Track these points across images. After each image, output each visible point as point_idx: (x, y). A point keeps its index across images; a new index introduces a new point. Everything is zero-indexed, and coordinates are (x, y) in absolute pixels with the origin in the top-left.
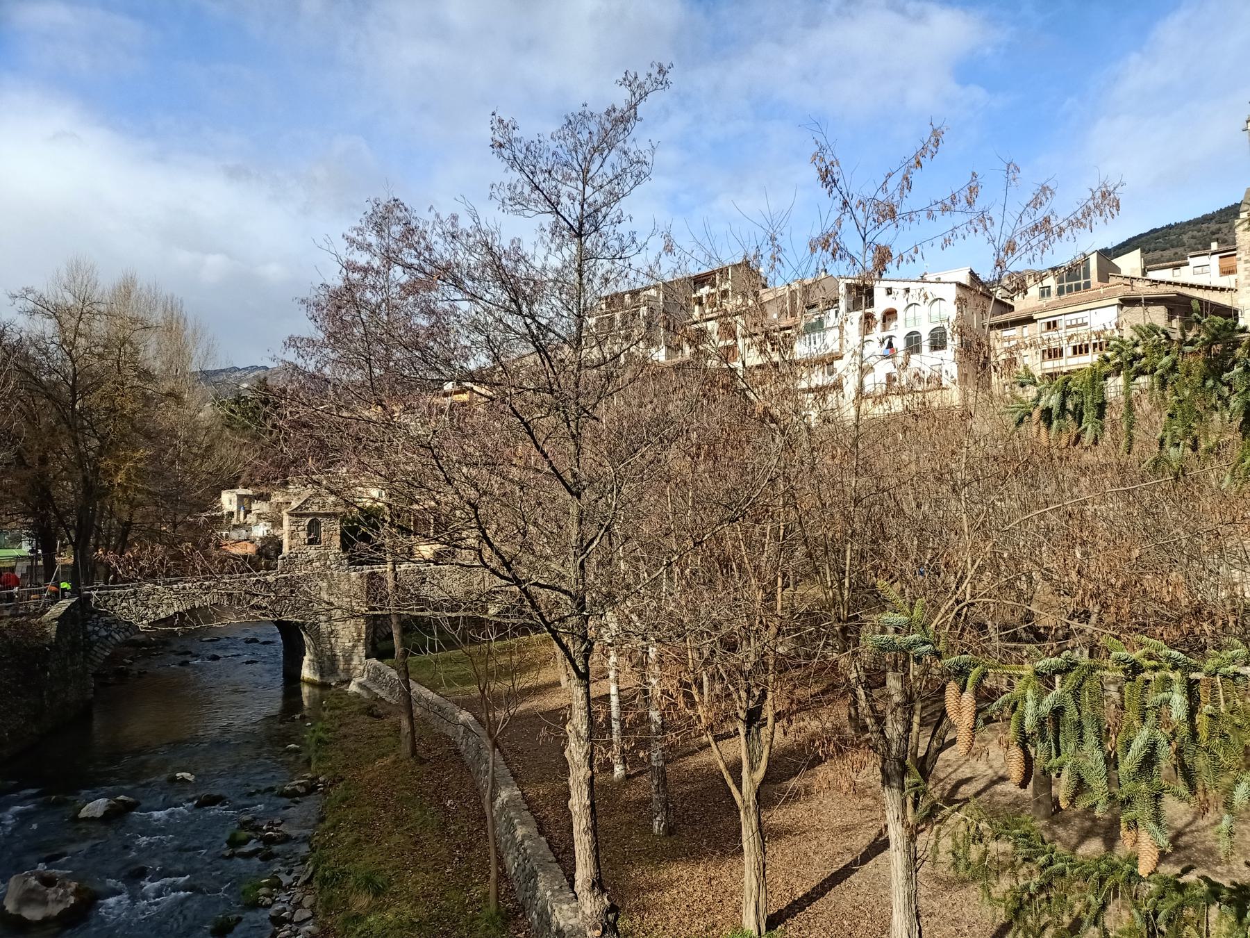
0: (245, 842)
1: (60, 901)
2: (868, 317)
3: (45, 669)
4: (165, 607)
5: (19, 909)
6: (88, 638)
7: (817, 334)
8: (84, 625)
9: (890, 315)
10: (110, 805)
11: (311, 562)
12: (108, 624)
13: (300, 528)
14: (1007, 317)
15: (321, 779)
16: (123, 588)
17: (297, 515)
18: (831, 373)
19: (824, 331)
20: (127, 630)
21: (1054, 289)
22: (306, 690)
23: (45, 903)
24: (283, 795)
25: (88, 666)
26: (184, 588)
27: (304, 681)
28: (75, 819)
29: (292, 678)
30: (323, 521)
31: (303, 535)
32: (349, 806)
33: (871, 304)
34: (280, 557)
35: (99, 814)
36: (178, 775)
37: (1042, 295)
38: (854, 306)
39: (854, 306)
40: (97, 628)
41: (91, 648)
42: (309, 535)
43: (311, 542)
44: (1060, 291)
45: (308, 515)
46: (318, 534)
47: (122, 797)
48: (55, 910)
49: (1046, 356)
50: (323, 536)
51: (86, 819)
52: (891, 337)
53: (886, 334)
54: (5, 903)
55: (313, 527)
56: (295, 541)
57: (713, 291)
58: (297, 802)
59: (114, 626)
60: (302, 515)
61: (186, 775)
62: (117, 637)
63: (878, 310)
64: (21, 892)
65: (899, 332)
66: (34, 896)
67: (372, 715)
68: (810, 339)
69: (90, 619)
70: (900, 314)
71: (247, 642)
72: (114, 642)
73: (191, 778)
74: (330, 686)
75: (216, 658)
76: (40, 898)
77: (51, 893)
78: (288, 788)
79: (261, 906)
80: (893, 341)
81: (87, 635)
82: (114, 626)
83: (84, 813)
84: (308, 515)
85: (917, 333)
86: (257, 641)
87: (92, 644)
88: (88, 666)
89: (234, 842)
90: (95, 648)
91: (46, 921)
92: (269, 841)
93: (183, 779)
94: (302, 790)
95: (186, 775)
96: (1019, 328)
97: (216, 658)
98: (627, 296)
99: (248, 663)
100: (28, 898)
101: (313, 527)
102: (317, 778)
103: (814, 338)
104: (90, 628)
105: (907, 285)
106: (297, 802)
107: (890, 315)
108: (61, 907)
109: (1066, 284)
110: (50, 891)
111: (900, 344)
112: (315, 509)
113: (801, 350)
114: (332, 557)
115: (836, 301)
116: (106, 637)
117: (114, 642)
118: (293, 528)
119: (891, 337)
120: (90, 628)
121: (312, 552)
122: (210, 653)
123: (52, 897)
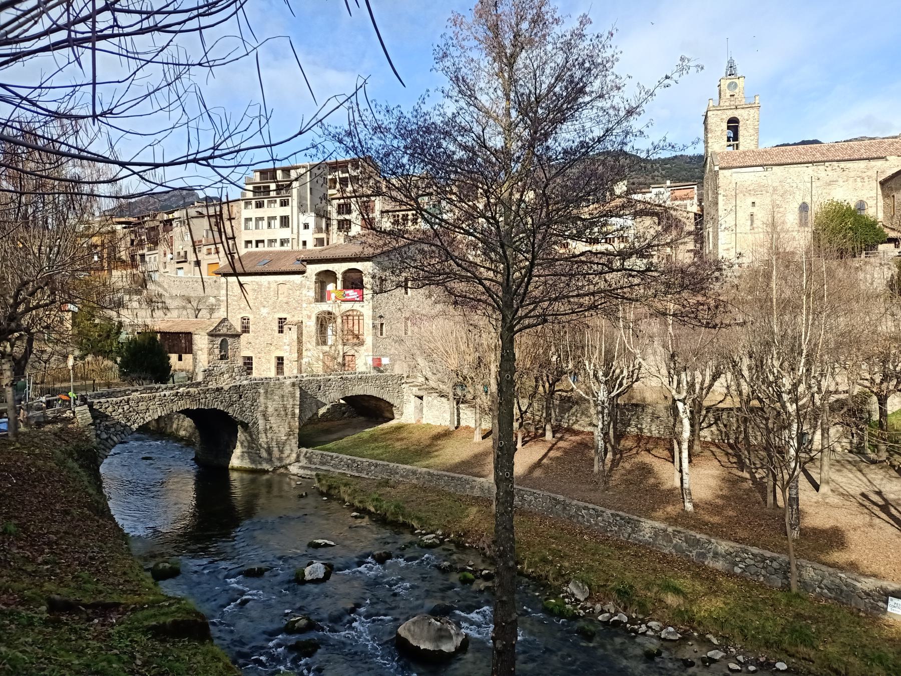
0: (472, 582)
11: (222, 373)
12: (107, 428)
20: (123, 433)
22: (234, 476)
23: (450, 637)
26: (165, 395)
30: (230, 341)
31: (217, 351)
43: (223, 358)
45: (220, 336)
46: (226, 351)
50: (230, 353)
51: (313, 581)
59: (113, 430)
62: (115, 439)
66: (443, 633)
72: (112, 443)
73: (332, 543)
76: (447, 634)
83: (308, 577)
84: (220, 336)
93: (326, 545)
108: (460, 639)
112: (224, 331)
116: (106, 439)
117: (112, 443)
118: (211, 346)
121: (223, 365)
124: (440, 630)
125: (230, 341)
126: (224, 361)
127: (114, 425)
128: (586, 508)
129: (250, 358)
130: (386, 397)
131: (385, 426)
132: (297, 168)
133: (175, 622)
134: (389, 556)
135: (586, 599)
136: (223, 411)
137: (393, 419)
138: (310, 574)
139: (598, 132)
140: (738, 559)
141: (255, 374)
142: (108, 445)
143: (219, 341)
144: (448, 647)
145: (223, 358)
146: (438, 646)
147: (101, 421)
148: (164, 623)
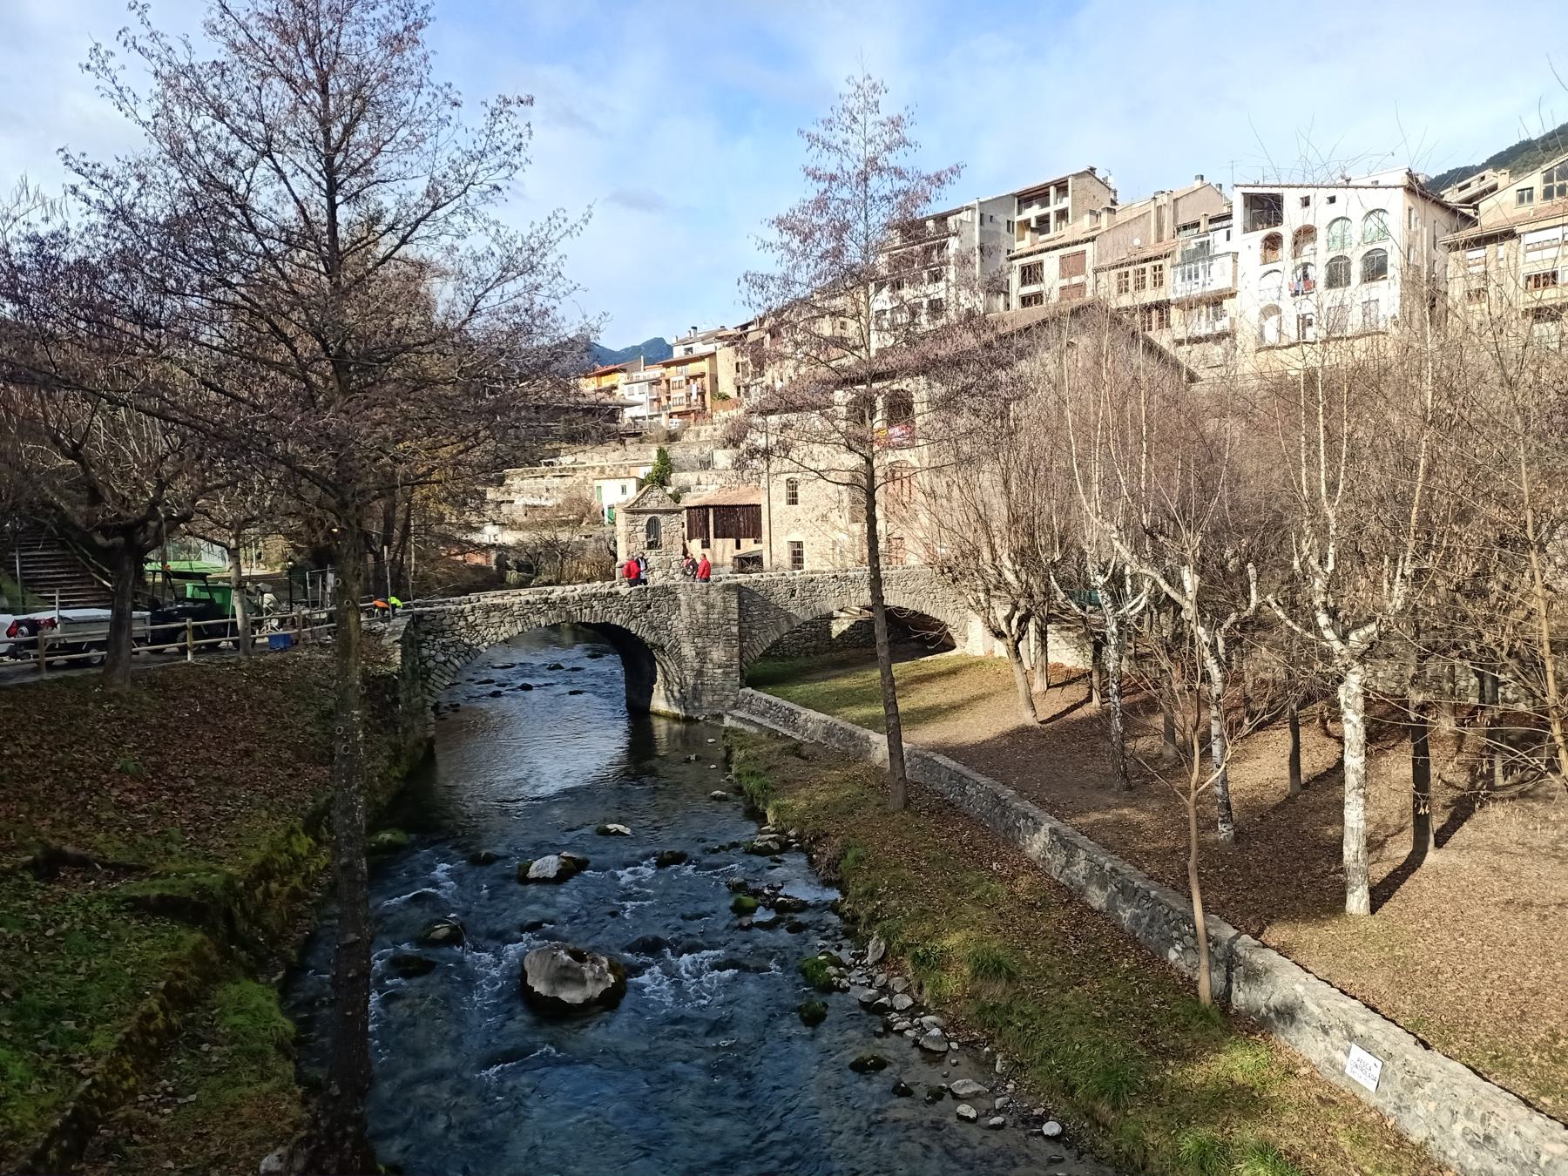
0: (752, 910)
1: (599, 980)
2: (1273, 243)
3: (396, 701)
4: (507, 625)
5: (554, 991)
6: (424, 663)
7: (1200, 264)
8: (420, 648)
9: (1306, 233)
10: (564, 864)
12: (445, 647)
13: (638, 529)
14: (1471, 232)
15: (792, 833)
16: (443, 603)
17: (633, 512)
18: (1217, 317)
19: (1211, 258)
20: (467, 654)
21: (1538, 191)
23: (582, 982)
24: (760, 852)
25: (427, 697)
27: (657, 714)
28: (524, 880)
29: (639, 713)
30: (663, 519)
31: (642, 536)
32: (871, 868)
33: (1278, 220)
34: (618, 564)
35: (552, 874)
36: (610, 826)
37: (1521, 199)
38: (1251, 227)
39: (1251, 227)
40: (433, 652)
41: (429, 676)
42: (648, 537)
43: (651, 546)
44: (1548, 194)
47: (565, 854)
48: (594, 990)
49: (1532, 283)
50: (664, 539)
51: (537, 881)
52: (1305, 266)
53: (1299, 261)
54: (529, 982)
55: (653, 527)
56: (633, 544)
57: (1044, 211)
58: (779, 861)
60: (639, 512)
61: (621, 827)
62: (456, 662)
63: (1286, 230)
64: (553, 970)
65: (1319, 256)
66: (569, 974)
67: (799, 756)
68: (1183, 273)
69: (423, 641)
70: (1322, 234)
71: (550, 669)
72: (453, 668)
73: (628, 831)
74: (697, 721)
75: (527, 688)
76: (577, 976)
77: (588, 971)
78: (759, 844)
79: (837, 989)
80: (1310, 270)
81: (423, 660)
82: (453, 649)
83: (532, 873)
85: (1346, 258)
86: (562, 668)
87: (429, 671)
88: (427, 697)
89: (740, 910)
90: (433, 676)
91: (589, 1003)
92: (782, 908)
93: (618, 832)
94: (776, 846)
95: (621, 827)
96: (1491, 247)
97: (527, 688)
98: (930, 224)
99: (572, 693)
100: (565, 976)
101: (653, 527)
102: (783, 832)
103: (1197, 270)
104: (425, 652)
105: (1332, 192)
106: (779, 861)
107: (1306, 233)
108: (602, 987)
109: (1557, 184)
110: (586, 967)
111: (1319, 274)
113: (1175, 287)
114: (674, 564)
115: (1229, 217)
116: (444, 663)
117: (453, 668)
118: (631, 529)
119: (1305, 266)
120: (425, 652)
122: (521, 682)
123: (588, 975)
124: (567, 967)
125: (663, 519)
126: (654, 552)
127: (454, 644)
128: (1026, 816)
129: (799, 544)
130: (928, 609)
131: (950, 653)
132: (959, 212)
133: (161, 897)
134: (679, 858)
135: (876, 963)
136: (620, 627)
137: (954, 647)
138: (537, 869)
139: (258, 208)
140: (1175, 934)
141: (807, 566)
142: (447, 670)
143: (645, 519)
144: (572, 995)
145: (651, 546)
146: (554, 991)
147: (436, 637)
148: (148, 897)
